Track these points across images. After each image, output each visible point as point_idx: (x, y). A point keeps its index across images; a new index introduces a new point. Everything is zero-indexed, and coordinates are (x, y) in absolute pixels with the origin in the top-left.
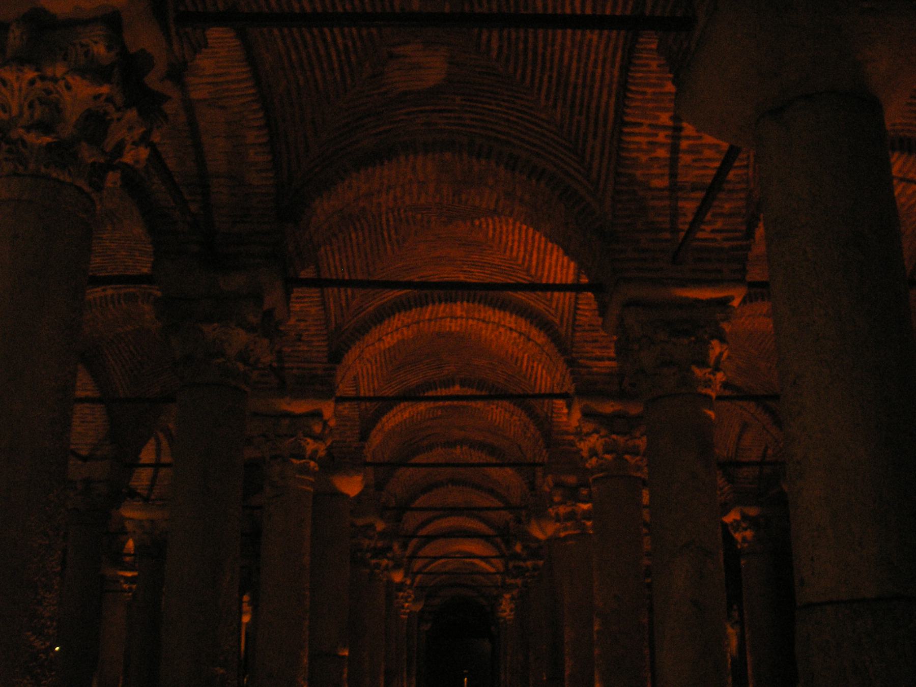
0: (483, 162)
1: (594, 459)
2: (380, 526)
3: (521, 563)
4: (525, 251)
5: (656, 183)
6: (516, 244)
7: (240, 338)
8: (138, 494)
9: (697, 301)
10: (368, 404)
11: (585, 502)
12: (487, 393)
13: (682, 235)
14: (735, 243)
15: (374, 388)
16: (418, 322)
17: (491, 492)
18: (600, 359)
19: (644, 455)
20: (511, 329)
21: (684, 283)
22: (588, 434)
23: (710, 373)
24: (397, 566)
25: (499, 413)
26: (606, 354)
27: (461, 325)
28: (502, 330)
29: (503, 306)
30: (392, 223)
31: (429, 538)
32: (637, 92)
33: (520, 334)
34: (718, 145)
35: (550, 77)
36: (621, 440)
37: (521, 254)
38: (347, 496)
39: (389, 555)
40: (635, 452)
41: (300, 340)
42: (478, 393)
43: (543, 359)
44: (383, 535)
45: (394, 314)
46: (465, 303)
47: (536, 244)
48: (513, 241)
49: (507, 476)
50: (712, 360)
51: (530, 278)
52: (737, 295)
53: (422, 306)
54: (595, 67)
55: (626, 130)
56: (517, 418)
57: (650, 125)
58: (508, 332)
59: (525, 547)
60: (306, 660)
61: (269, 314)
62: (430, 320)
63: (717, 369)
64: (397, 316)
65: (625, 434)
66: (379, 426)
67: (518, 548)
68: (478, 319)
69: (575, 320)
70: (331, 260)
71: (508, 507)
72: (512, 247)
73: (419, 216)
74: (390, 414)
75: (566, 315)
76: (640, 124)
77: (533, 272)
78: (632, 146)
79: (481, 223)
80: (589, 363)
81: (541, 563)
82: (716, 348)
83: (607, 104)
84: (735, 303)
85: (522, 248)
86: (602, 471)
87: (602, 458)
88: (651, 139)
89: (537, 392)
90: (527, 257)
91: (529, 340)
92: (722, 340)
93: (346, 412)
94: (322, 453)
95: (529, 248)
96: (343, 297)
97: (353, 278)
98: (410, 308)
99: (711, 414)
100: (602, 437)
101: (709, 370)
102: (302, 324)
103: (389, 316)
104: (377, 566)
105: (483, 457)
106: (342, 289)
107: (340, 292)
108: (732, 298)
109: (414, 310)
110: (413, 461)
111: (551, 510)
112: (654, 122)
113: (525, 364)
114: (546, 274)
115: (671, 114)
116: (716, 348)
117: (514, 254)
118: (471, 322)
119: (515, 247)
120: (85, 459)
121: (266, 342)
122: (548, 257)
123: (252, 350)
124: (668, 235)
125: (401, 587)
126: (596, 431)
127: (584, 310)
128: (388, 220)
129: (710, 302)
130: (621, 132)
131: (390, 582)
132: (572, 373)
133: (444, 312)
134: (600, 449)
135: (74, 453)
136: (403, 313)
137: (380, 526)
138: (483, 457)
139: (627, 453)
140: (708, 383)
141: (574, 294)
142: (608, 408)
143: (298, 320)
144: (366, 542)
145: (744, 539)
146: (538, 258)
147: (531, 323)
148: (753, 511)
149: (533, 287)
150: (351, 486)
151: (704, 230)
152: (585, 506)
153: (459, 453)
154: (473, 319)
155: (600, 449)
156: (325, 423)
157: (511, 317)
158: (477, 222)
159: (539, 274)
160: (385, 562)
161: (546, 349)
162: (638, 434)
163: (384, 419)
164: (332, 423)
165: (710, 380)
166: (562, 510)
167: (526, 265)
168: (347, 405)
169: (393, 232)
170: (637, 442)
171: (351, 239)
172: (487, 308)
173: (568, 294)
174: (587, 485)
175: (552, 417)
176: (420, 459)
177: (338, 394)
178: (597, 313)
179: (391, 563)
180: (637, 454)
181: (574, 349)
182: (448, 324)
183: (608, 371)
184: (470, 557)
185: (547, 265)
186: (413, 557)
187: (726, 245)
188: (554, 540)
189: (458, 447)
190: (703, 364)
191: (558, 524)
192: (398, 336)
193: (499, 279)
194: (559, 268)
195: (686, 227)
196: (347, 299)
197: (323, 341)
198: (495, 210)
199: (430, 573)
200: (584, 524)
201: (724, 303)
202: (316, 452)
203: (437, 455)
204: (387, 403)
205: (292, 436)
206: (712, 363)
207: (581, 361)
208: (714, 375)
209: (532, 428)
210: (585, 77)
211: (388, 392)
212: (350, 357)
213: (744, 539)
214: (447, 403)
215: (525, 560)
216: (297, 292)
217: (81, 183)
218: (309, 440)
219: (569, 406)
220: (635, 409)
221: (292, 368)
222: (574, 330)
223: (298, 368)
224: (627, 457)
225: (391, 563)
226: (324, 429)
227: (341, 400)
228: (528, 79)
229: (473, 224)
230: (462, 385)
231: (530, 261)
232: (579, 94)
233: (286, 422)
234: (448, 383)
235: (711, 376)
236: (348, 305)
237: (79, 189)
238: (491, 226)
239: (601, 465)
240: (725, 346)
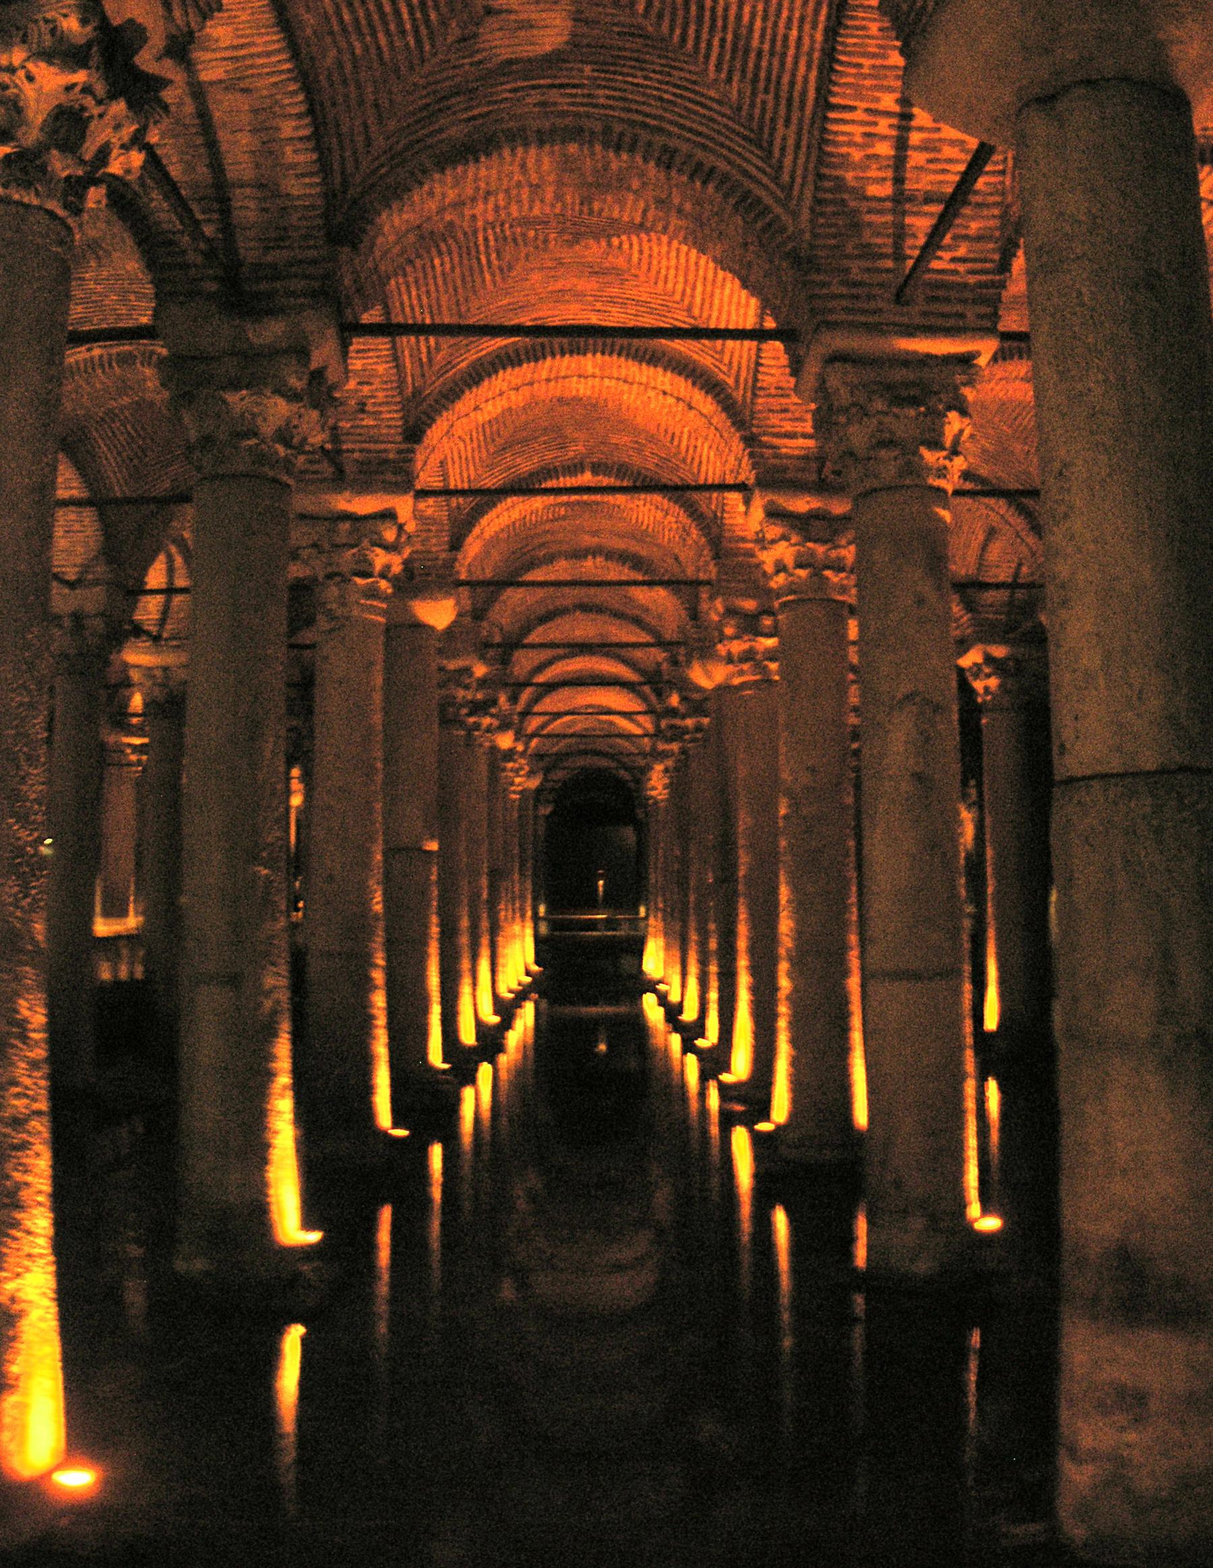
0: (625, 156)
1: (781, 579)
2: (480, 670)
3: (677, 722)
4: (686, 282)
5: (873, 190)
6: (672, 272)
7: (278, 409)
8: (148, 633)
9: (929, 356)
10: (461, 500)
12: (630, 484)
13: (910, 263)
14: (984, 278)
15: (469, 477)
16: (531, 384)
17: (637, 621)
18: (791, 436)
19: (852, 571)
20: (665, 393)
21: (910, 331)
22: (773, 542)
23: (945, 458)
24: (504, 726)
25: (649, 513)
26: (799, 429)
27: (593, 387)
28: (651, 393)
29: (653, 359)
30: (492, 243)
31: (551, 687)
32: (849, 64)
33: (678, 399)
34: (963, 142)
35: (723, 40)
36: (820, 549)
37: (680, 287)
38: (432, 628)
39: (493, 710)
40: (839, 567)
41: (363, 411)
42: (618, 483)
43: (711, 436)
44: (483, 683)
45: (496, 372)
46: (599, 355)
47: (701, 272)
48: (668, 268)
49: (658, 600)
51: (692, 321)
52: (985, 348)
53: (536, 360)
54: (788, 27)
55: (832, 115)
56: (673, 520)
57: (867, 110)
58: (661, 397)
59: (684, 699)
60: (379, 857)
61: (318, 376)
62: (548, 380)
63: (955, 452)
64: (501, 372)
65: (825, 542)
66: (476, 531)
67: (674, 700)
68: (618, 379)
69: (756, 380)
70: (405, 297)
71: (661, 643)
72: (666, 277)
73: (532, 234)
74: (492, 514)
75: (743, 374)
76: (852, 109)
77: (696, 312)
78: (841, 138)
79: (621, 244)
80: (776, 441)
81: (706, 721)
82: (954, 423)
83: (806, 79)
84: (982, 361)
85: (681, 279)
86: (795, 592)
87: (791, 575)
88: (868, 129)
89: (701, 482)
90: (688, 290)
91: (690, 408)
92: (964, 412)
93: (430, 512)
94: (397, 569)
95: (691, 277)
96: (424, 350)
97: (438, 321)
98: (520, 364)
99: (946, 515)
100: (792, 545)
101: (944, 453)
102: (366, 389)
103: (490, 376)
104: (477, 726)
105: (626, 573)
106: (422, 338)
107: (418, 342)
108: (978, 354)
109: (525, 365)
110: (529, 577)
111: (719, 646)
112: (873, 106)
113: (684, 443)
114: (715, 314)
115: (897, 95)
116: (954, 423)
117: (670, 285)
118: (607, 382)
119: (671, 276)
121: (315, 414)
122: (718, 291)
123: (295, 427)
124: (889, 264)
125: (510, 755)
126: (784, 537)
127: (769, 366)
128: (486, 239)
129: (948, 359)
130: (825, 118)
131: (494, 749)
132: (751, 455)
133: (568, 368)
134: (789, 561)
136: (509, 370)
137: (480, 670)
138: (626, 573)
139: (828, 568)
140: (942, 472)
141: (754, 344)
142: (802, 504)
143: (359, 383)
144: (461, 693)
145: (986, 689)
146: (703, 293)
147: (694, 384)
149: (696, 333)
150: (438, 613)
151: (940, 258)
152: (771, 642)
153: (591, 567)
154: (610, 378)
155: (789, 561)
156: (401, 528)
157: (664, 376)
158: (615, 241)
159: (705, 315)
160: (486, 721)
161: (714, 421)
162: (843, 542)
163: (484, 521)
164: (411, 527)
165: (945, 468)
166: (737, 647)
167: (686, 302)
168: (431, 501)
169: (494, 256)
170: (843, 552)
171: (433, 267)
172: (630, 362)
173: (747, 343)
174: (770, 612)
175: (722, 518)
176: (537, 575)
177: (418, 487)
178: (788, 370)
179: (496, 723)
180: (841, 569)
181: (754, 422)
182: (574, 385)
183: (803, 452)
184: (605, 714)
185: (716, 302)
186: (526, 713)
187: (972, 280)
188: (724, 689)
189: (590, 557)
190: (936, 445)
191: (730, 666)
192: (501, 404)
193: (648, 321)
194: (733, 307)
195: (916, 253)
196: (429, 352)
197: (396, 411)
198: (642, 225)
199: (548, 736)
200: (766, 666)
201: (966, 360)
202: (388, 567)
203: (561, 570)
204: (487, 497)
205: (357, 546)
206: (948, 444)
207: (764, 439)
208: (951, 460)
209: (695, 532)
210: (773, 41)
211: (490, 483)
212: (434, 434)
213: (986, 689)
214: (574, 498)
215: (684, 717)
216: (358, 343)
217: (53, 205)
218: (378, 550)
219: (747, 502)
220: (839, 507)
221: (353, 451)
222: (755, 395)
223: (361, 451)
224: (828, 573)
225: (496, 723)
226: (399, 535)
227: (423, 494)
228: (690, 43)
229: (610, 245)
230: (596, 469)
231: (693, 296)
232: (764, 64)
233: (345, 526)
234: (575, 468)
235: (947, 462)
236: (430, 360)
237: (51, 214)
238: (636, 247)
239: (792, 583)
240: (967, 421)
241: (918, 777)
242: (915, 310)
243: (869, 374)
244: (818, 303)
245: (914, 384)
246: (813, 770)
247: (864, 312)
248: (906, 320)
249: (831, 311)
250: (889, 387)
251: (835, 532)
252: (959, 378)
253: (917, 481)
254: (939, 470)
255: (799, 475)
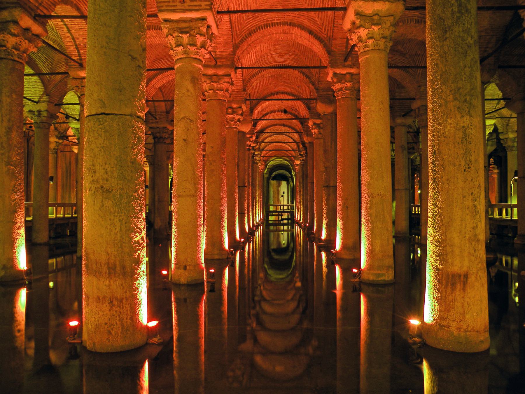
11: (230, 114)
21: (184, 11)
36: (215, 85)
50: (199, 45)
65: (216, 82)
92: (201, 35)
101: (196, 48)
102: (85, 40)
120: (37, 102)
129: (197, 19)
134: (208, 89)
135: (25, 98)
142: (210, 72)
145: (315, 132)
148: (318, 121)
152: (231, 116)
155: (208, 89)
165: (198, 52)
170: (222, 85)
180: (222, 90)
190: (195, 45)
213: (315, 132)
220: (221, 72)
241: (185, 140)
242: (186, 5)
243: (175, 25)
244: (159, 5)
245: (188, 27)
246: (212, 147)
247: (171, 6)
248: (182, 8)
249: (162, 6)
250: (180, 29)
251: (220, 79)
252: (200, 25)
253: (189, 56)
254: (195, 52)
255: (209, 63)
